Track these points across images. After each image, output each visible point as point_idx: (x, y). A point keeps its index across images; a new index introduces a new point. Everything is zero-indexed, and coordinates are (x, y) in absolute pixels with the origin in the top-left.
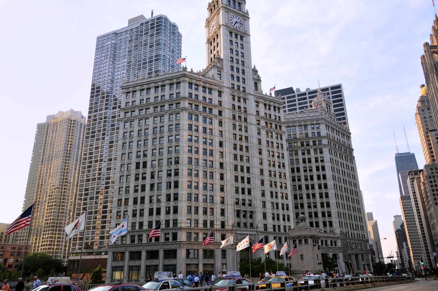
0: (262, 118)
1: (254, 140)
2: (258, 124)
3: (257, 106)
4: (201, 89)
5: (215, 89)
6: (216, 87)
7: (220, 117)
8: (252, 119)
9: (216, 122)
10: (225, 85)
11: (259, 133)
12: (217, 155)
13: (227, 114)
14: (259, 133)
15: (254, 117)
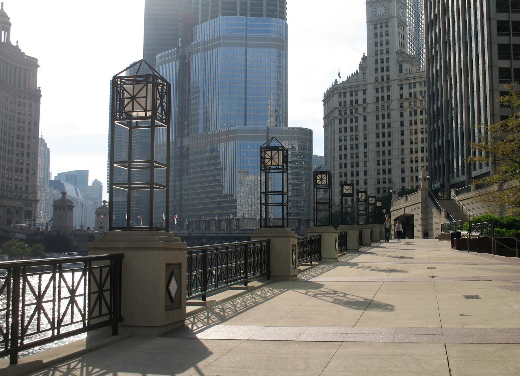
0: (406, 100)
1: (396, 125)
2: (402, 107)
3: (401, 88)
4: (348, 95)
5: (359, 90)
6: (360, 88)
7: (365, 113)
8: (395, 105)
9: (361, 119)
10: (369, 82)
11: (402, 115)
12: (361, 148)
13: (371, 108)
14: (402, 115)
15: (396, 102)
